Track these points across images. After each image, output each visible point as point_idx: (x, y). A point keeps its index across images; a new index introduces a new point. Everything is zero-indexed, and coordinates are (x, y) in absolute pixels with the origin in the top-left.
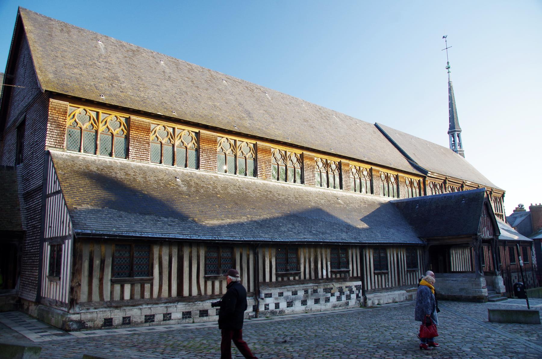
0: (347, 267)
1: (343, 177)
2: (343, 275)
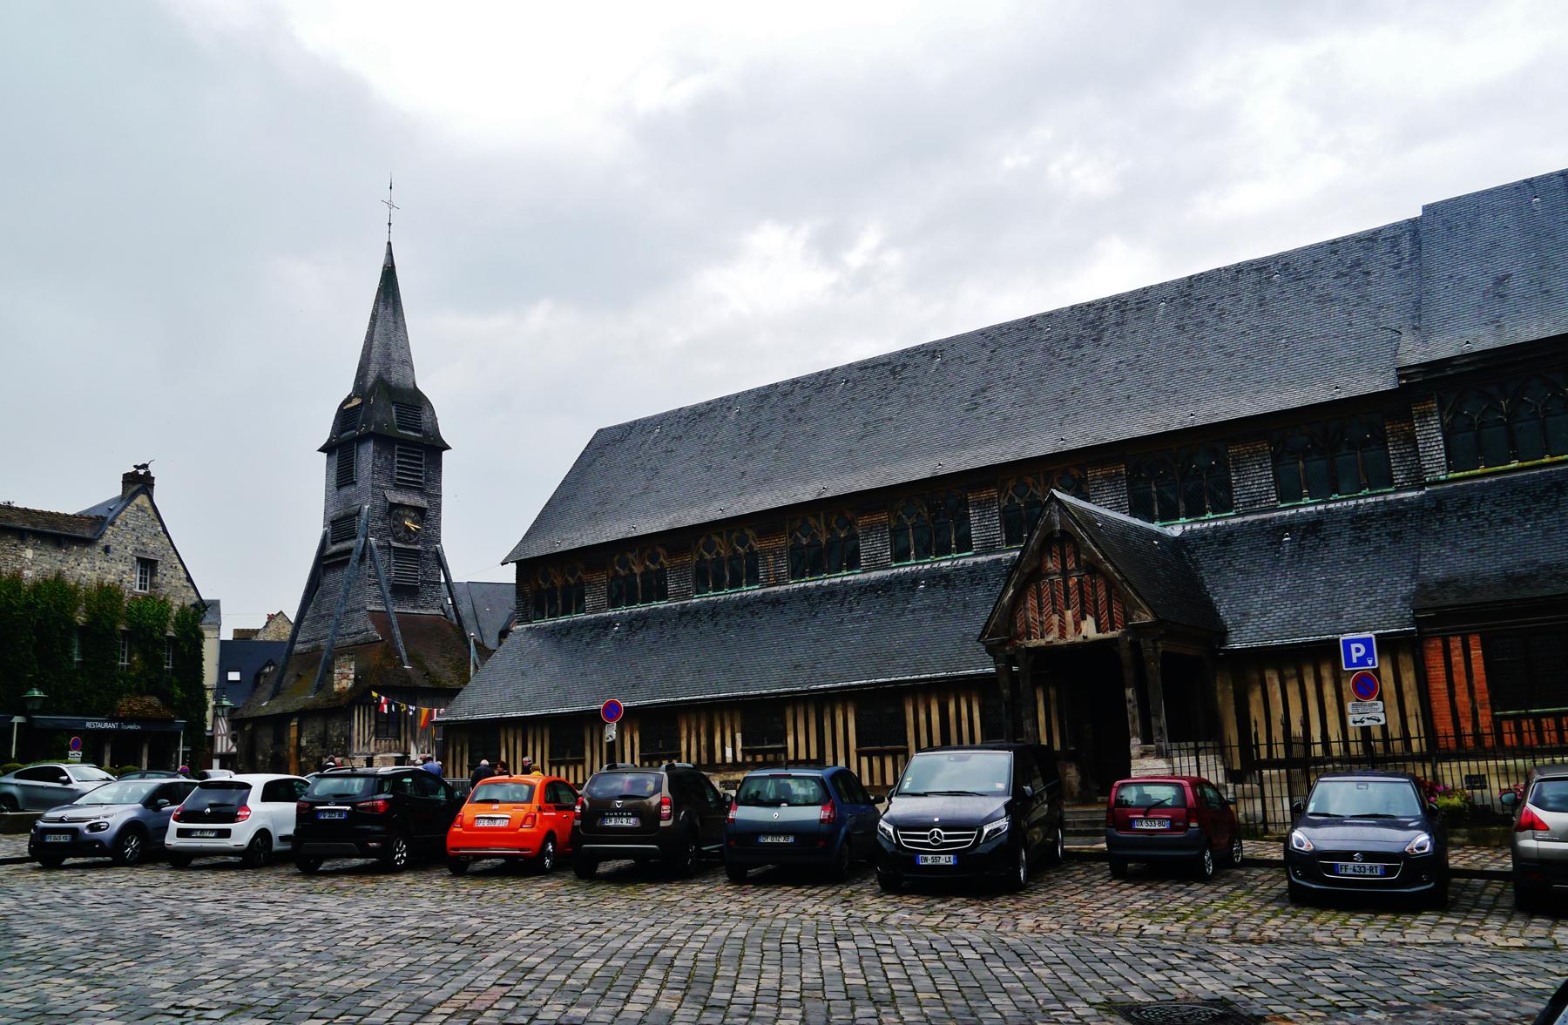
0: (784, 739)
1: (974, 519)
2: (770, 757)
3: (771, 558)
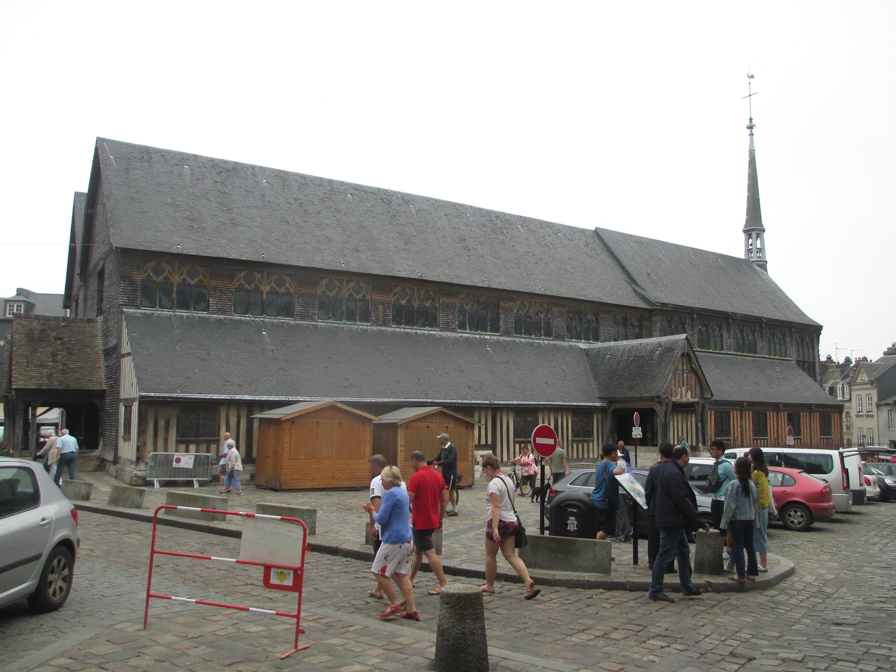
3: (381, 307)
